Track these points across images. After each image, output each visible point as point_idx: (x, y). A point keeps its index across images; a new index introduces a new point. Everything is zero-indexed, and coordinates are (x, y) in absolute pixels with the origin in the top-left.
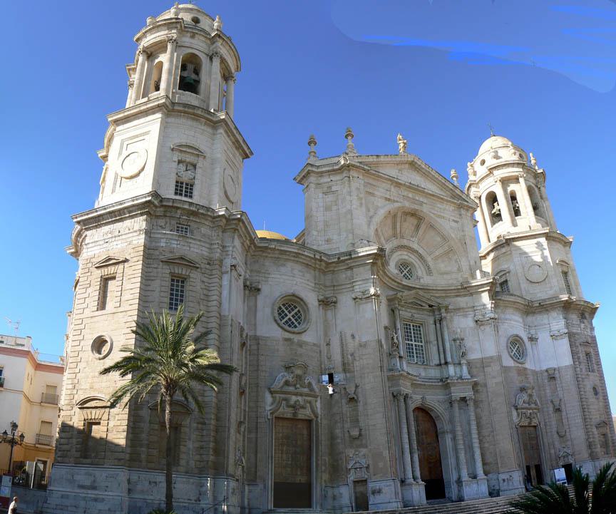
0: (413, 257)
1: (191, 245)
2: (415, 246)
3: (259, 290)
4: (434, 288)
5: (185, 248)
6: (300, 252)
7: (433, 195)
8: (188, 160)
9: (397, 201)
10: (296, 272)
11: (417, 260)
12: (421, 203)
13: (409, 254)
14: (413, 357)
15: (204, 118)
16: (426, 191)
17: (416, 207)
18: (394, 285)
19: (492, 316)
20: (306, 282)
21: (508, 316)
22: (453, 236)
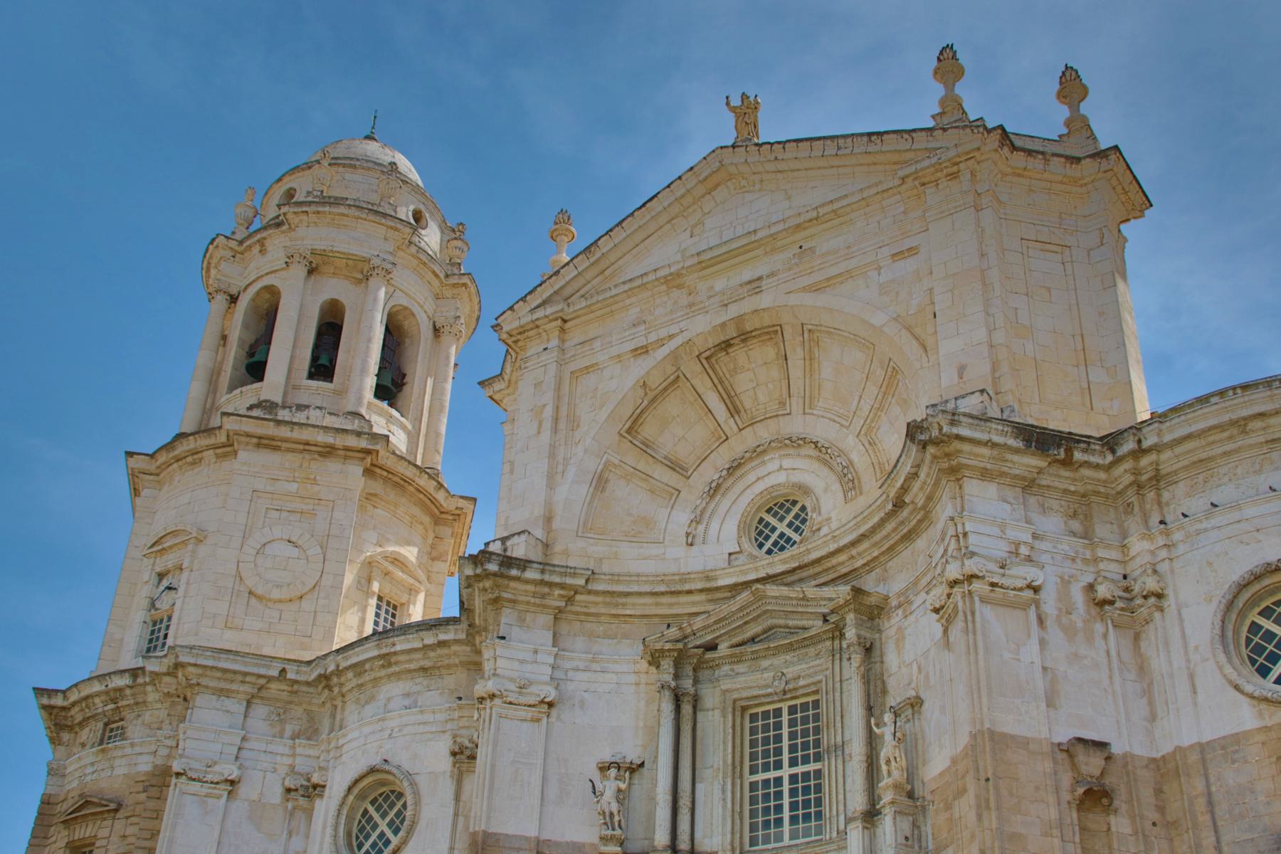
0: (799, 463)
1: (117, 762)
2: (796, 425)
3: (324, 786)
4: (833, 547)
5: (103, 774)
6: (384, 651)
7: (798, 227)
8: (170, 565)
9: (671, 337)
10: (392, 705)
11: (816, 465)
12: (755, 285)
13: (787, 463)
14: (779, 822)
15: (209, 448)
16: (760, 235)
17: (734, 311)
18: (694, 603)
19: (953, 571)
20: (420, 718)
21: (1223, 494)
22: (878, 319)
